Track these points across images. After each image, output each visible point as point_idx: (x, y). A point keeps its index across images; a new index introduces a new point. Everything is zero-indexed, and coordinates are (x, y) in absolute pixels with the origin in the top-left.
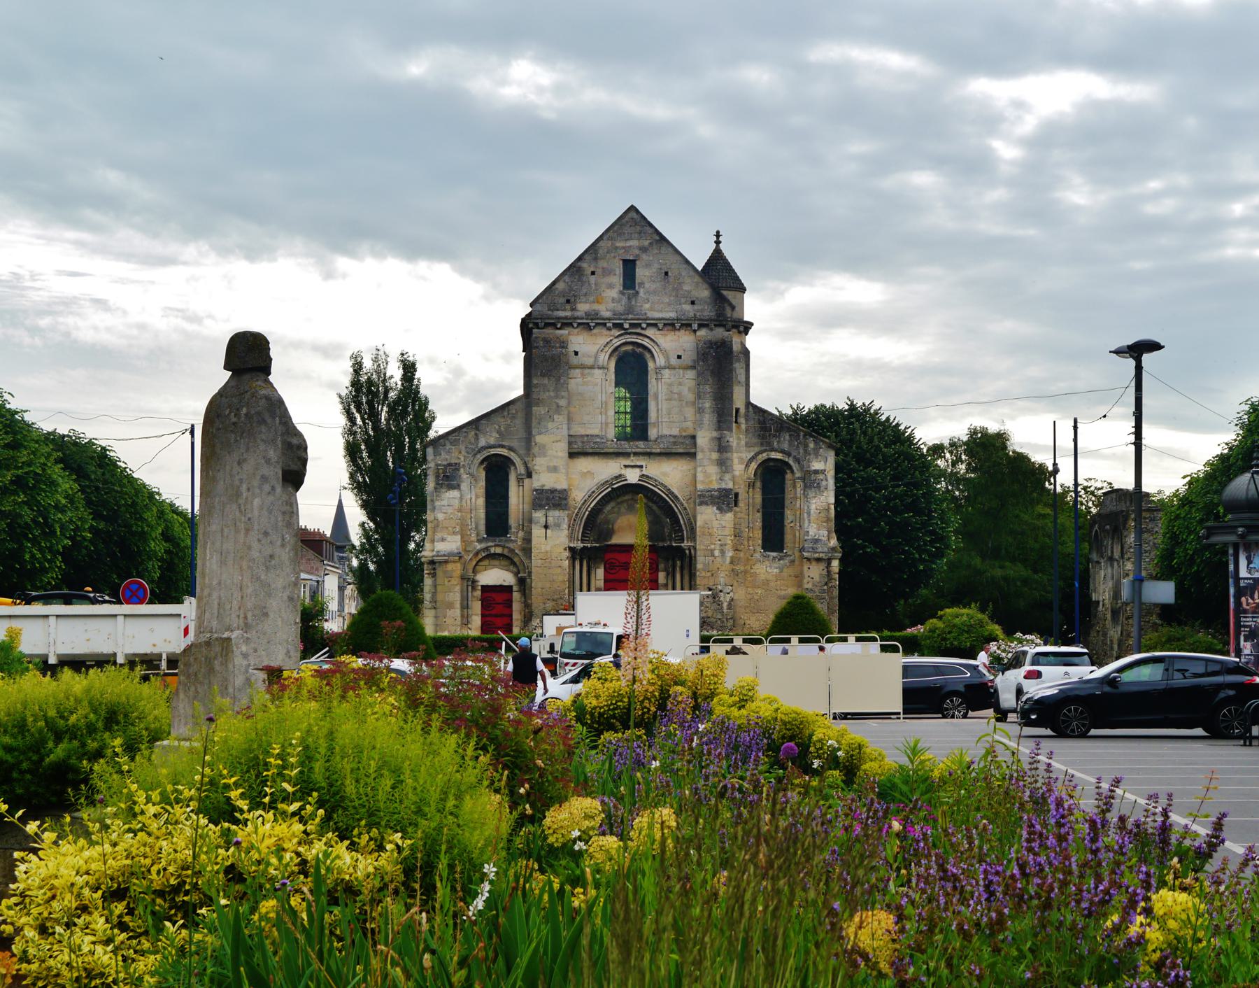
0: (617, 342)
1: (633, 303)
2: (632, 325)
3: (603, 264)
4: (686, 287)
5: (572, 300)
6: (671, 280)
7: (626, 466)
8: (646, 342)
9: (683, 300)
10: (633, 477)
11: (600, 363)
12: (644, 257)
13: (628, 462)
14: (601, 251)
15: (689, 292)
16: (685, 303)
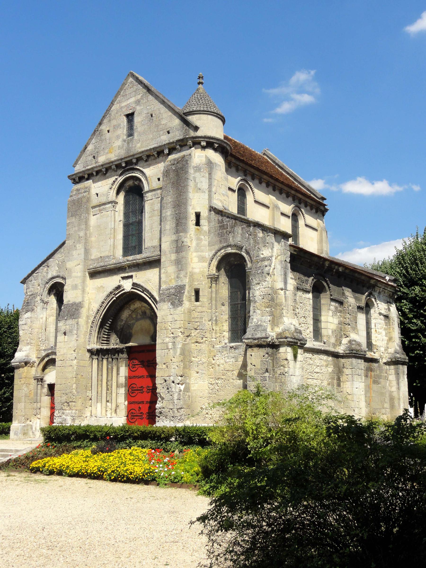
0: (121, 179)
1: (130, 146)
2: (127, 163)
3: (114, 122)
4: (163, 122)
5: (96, 156)
6: (154, 118)
7: (123, 278)
8: (137, 175)
9: (161, 133)
10: (127, 286)
11: (110, 199)
12: (138, 108)
13: (123, 275)
14: (113, 114)
15: (166, 125)
16: (163, 134)
